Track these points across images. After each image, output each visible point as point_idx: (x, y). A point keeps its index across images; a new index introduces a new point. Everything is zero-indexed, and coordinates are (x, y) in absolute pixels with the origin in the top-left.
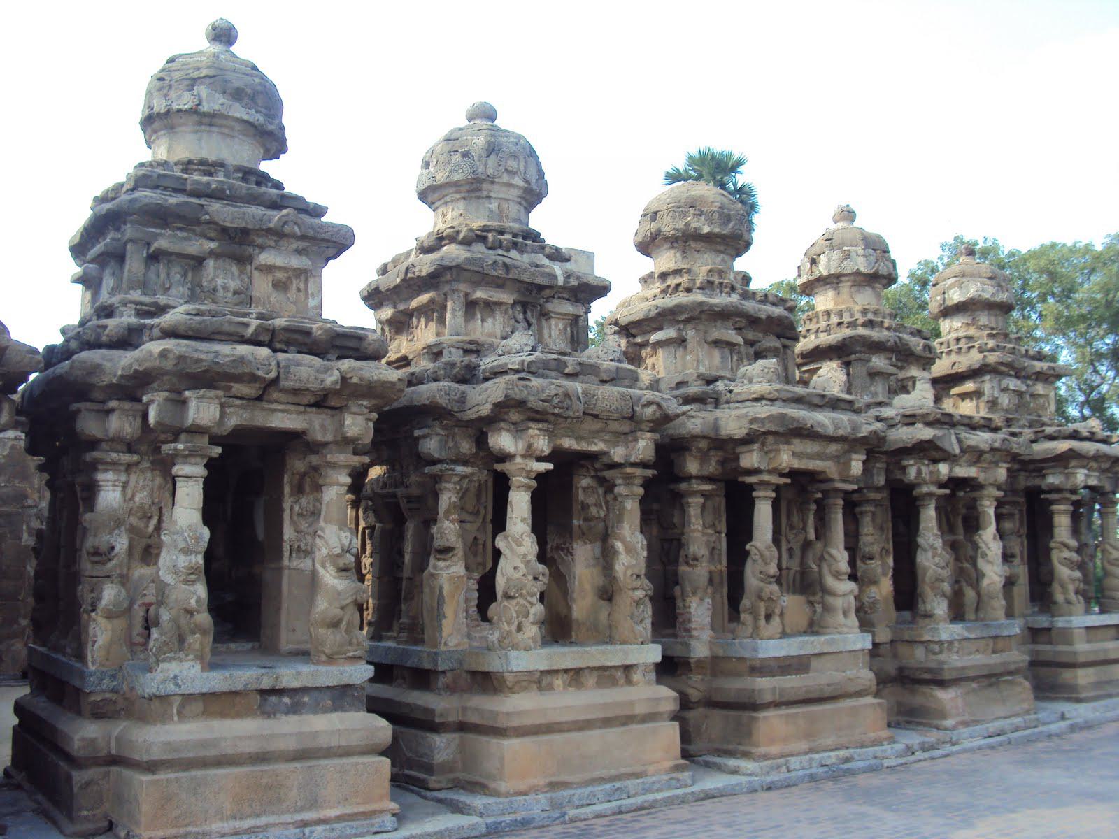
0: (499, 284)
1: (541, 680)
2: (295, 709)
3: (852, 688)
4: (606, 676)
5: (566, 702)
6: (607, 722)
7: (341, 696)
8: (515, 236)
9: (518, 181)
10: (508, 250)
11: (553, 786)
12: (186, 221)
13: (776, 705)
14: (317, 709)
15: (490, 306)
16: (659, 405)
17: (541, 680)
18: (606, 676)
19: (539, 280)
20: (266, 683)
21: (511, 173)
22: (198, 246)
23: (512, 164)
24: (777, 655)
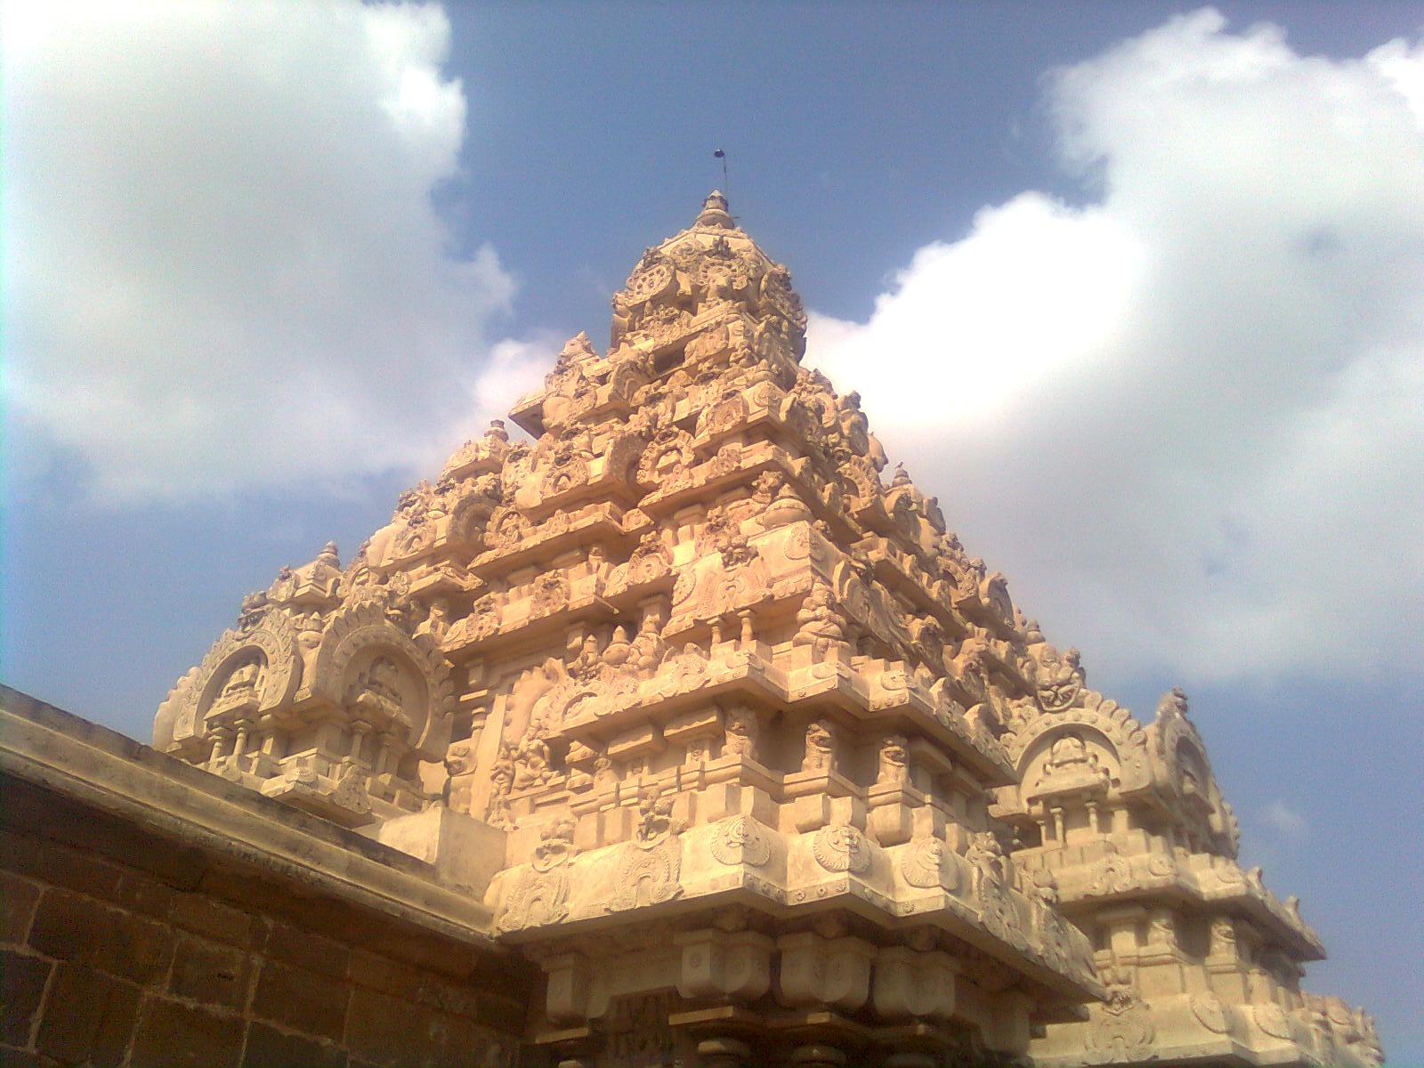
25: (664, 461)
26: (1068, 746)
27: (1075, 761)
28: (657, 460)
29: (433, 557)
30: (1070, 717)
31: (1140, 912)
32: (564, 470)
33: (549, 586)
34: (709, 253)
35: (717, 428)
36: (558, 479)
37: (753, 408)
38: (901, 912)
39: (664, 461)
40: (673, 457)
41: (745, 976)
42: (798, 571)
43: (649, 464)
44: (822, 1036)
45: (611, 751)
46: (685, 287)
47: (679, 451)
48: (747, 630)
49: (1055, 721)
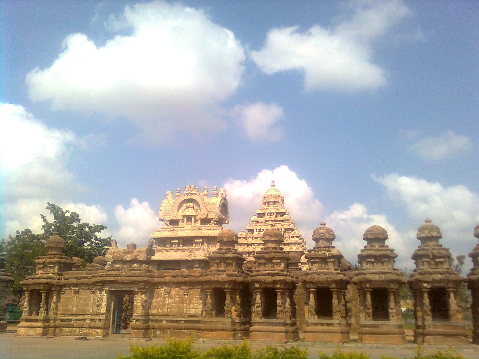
0: (317, 258)
1: (315, 324)
2: (272, 326)
3: (390, 332)
4: (328, 325)
5: (320, 328)
6: (326, 332)
7: (279, 324)
8: (323, 248)
9: (324, 238)
10: (318, 252)
11: (314, 341)
12: (262, 258)
13: (366, 333)
14: (276, 326)
15: (315, 262)
16: (333, 278)
17: (315, 324)
18: (328, 325)
19: (323, 256)
20: (268, 322)
21: (322, 236)
22: (263, 261)
23: (322, 235)
24: (368, 324)
35: (294, 235)
46: (275, 201)
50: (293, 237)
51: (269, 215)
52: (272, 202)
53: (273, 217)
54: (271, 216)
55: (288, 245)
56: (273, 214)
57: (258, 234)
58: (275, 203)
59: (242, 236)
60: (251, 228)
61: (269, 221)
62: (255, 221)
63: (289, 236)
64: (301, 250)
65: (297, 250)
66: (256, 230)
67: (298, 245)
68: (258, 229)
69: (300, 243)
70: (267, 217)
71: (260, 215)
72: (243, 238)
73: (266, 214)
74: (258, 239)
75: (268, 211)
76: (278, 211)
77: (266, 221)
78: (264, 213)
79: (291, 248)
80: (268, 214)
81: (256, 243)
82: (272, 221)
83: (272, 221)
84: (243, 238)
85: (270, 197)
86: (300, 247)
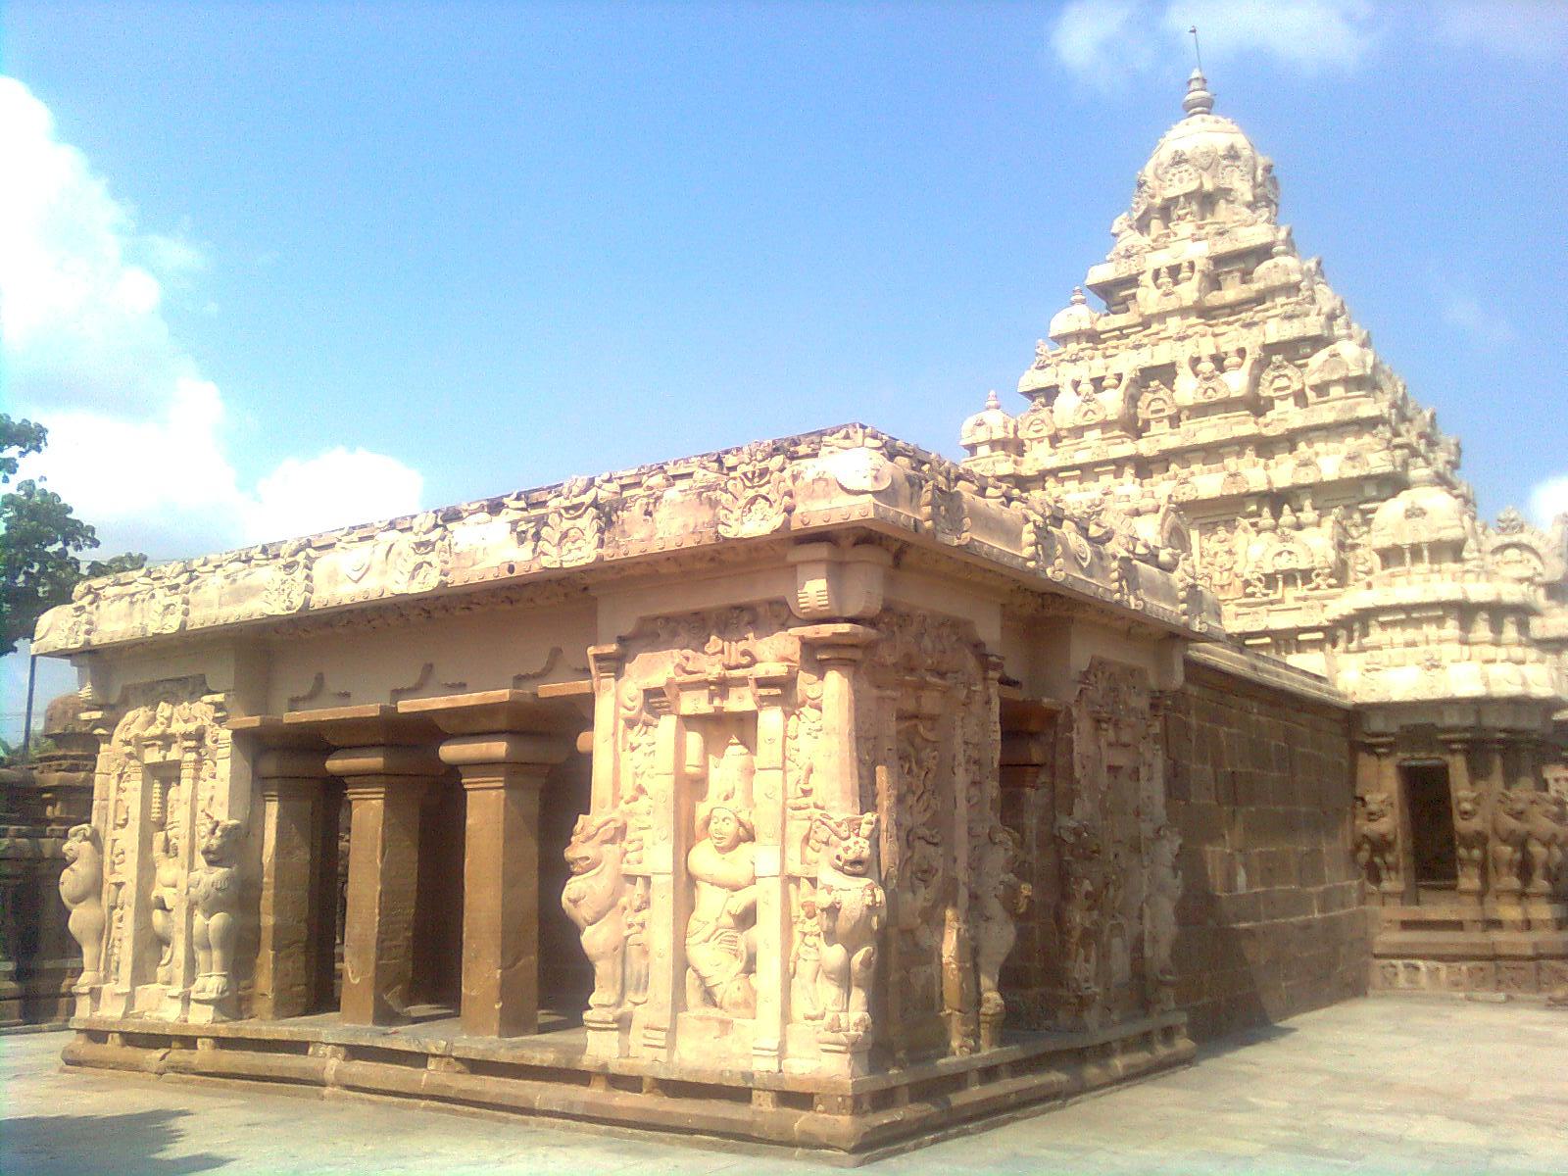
25: (1278, 383)
26: (1512, 553)
27: (1516, 562)
28: (1272, 382)
29: (1105, 425)
30: (1515, 538)
31: (1557, 646)
32: (1212, 385)
33: (1234, 475)
34: (1224, 157)
35: (1327, 377)
36: (1205, 392)
37: (1351, 367)
38: (1534, 696)
39: (1278, 383)
40: (1284, 382)
41: (1470, 721)
42: (1453, 527)
43: (1267, 384)
44: (1500, 741)
45: (1381, 619)
46: (1208, 186)
47: (1289, 379)
48: (1426, 553)
49: (1507, 540)
50: (1321, 389)
51: (1164, 279)
52: (1188, 196)
53: (1188, 292)
54: (1176, 283)
55: (1293, 449)
56: (1192, 266)
57: (1085, 407)
58: (1207, 201)
59: (982, 435)
60: (1043, 379)
61: (1161, 317)
62: (1077, 336)
63: (1296, 386)
64: (1379, 471)
65: (1354, 473)
66: (1076, 384)
67: (1358, 434)
68: (1085, 380)
69: (1369, 424)
70: (1149, 298)
71: (1114, 294)
72: (994, 444)
73: (1146, 279)
74: (1087, 435)
75: (1162, 259)
76: (1224, 246)
77: (1146, 323)
78: (1132, 281)
79: (1305, 464)
80: (1157, 274)
81: (1069, 463)
82: (1183, 312)
83: (1183, 312)
84: (994, 444)
85: (1173, 170)
86: (1373, 451)
